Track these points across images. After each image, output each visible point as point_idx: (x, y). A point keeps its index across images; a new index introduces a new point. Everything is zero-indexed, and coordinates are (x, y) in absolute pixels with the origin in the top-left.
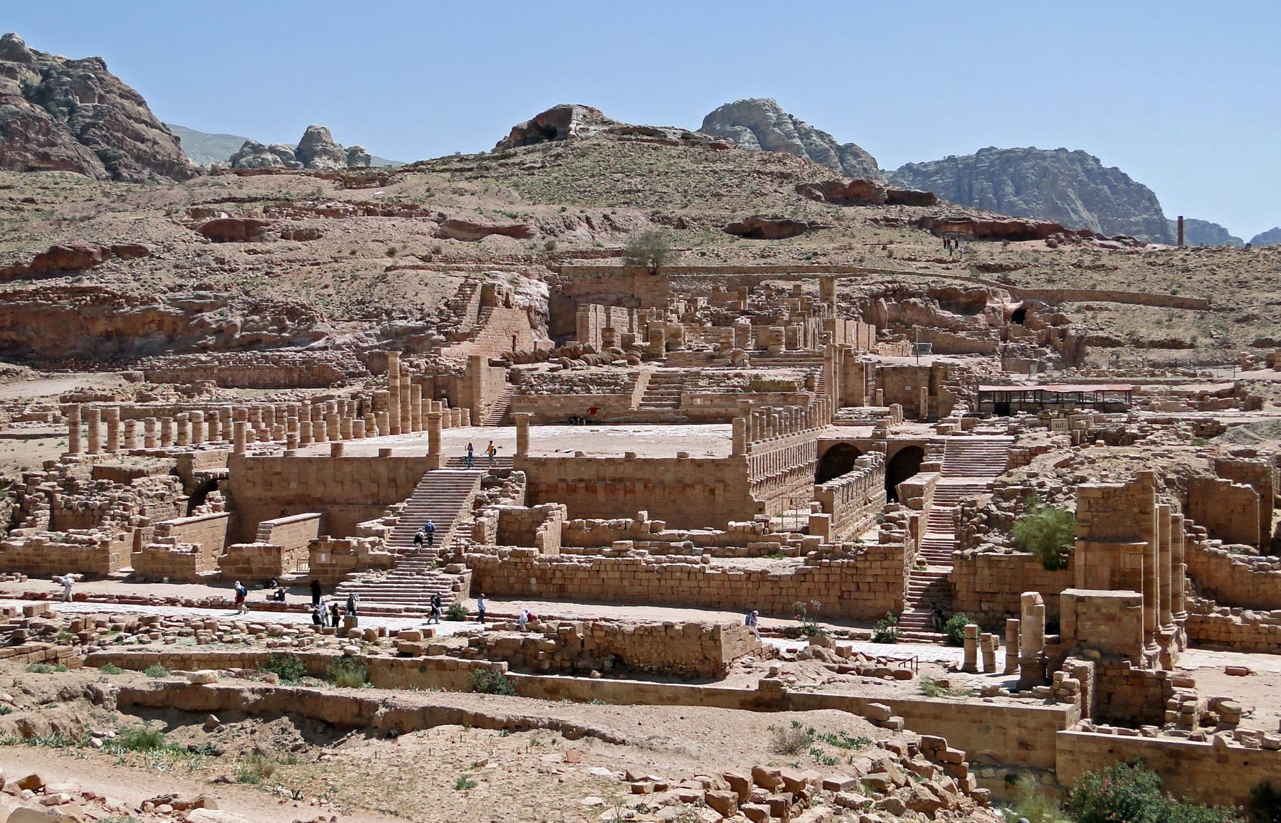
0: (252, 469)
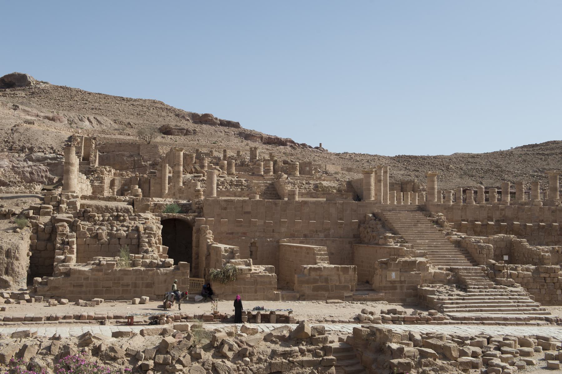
0: (225, 209)
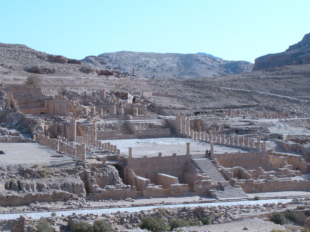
0: (136, 161)
